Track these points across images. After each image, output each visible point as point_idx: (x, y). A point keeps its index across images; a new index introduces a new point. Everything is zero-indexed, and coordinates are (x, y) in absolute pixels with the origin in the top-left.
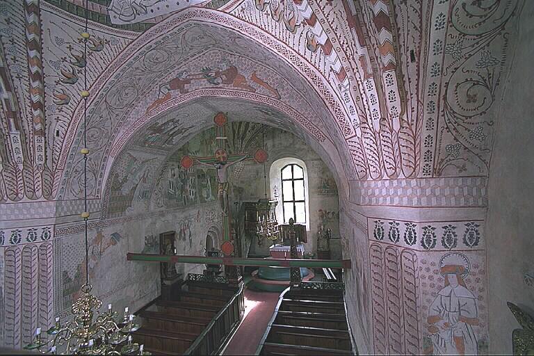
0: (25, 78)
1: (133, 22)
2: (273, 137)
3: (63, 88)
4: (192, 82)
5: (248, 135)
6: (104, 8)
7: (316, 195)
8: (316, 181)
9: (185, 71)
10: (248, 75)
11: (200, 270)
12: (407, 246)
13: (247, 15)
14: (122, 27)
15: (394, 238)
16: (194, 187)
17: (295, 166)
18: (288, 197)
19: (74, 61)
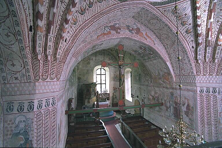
0: (65, 4)
2: (96, 56)
3: (77, 16)
7: (112, 81)
8: (113, 76)
10: (144, 33)
17: (102, 69)
19: (88, 3)
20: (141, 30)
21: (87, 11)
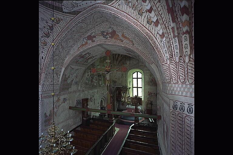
1: (72, 11)
4: (97, 37)
5: (119, 59)
6: (60, 5)
8: (148, 79)
9: (94, 32)
10: (120, 35)
11: (98, 114)
12: (188, 114)
13: (121, 7)
14: (68, 13)
15: (182, 110)
16: (96, 80)
17: (138, 73)
18: (135, 85)
19: (48, 28)
20: (117, 33)
21: (51, 34)
